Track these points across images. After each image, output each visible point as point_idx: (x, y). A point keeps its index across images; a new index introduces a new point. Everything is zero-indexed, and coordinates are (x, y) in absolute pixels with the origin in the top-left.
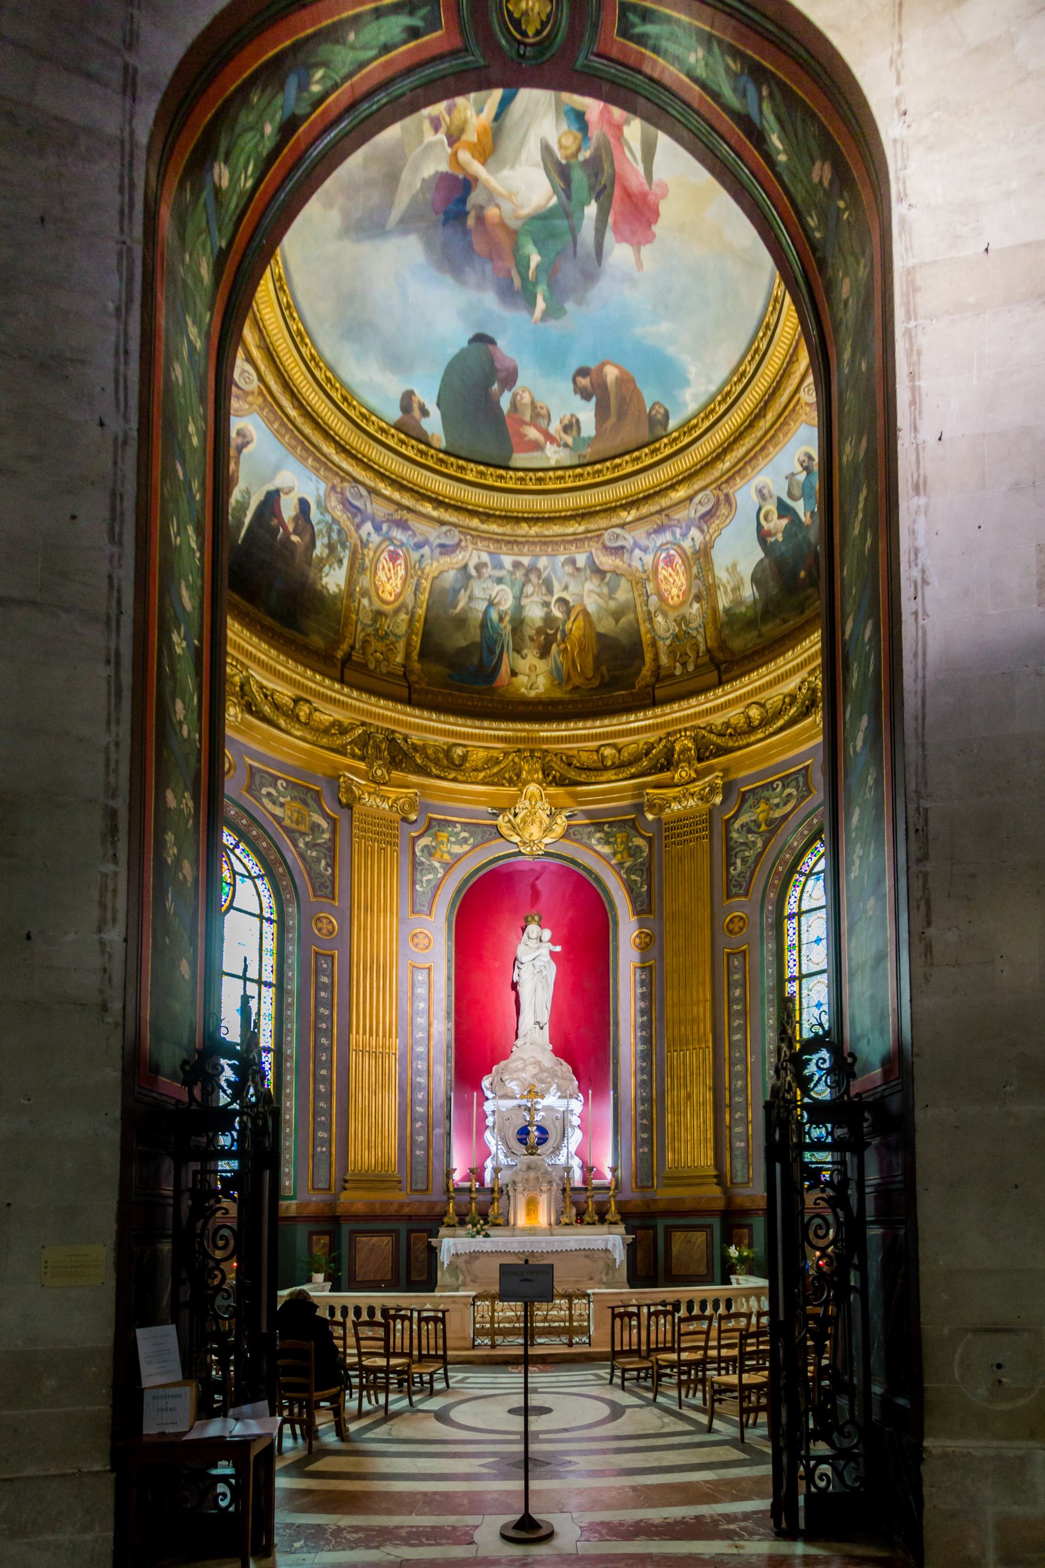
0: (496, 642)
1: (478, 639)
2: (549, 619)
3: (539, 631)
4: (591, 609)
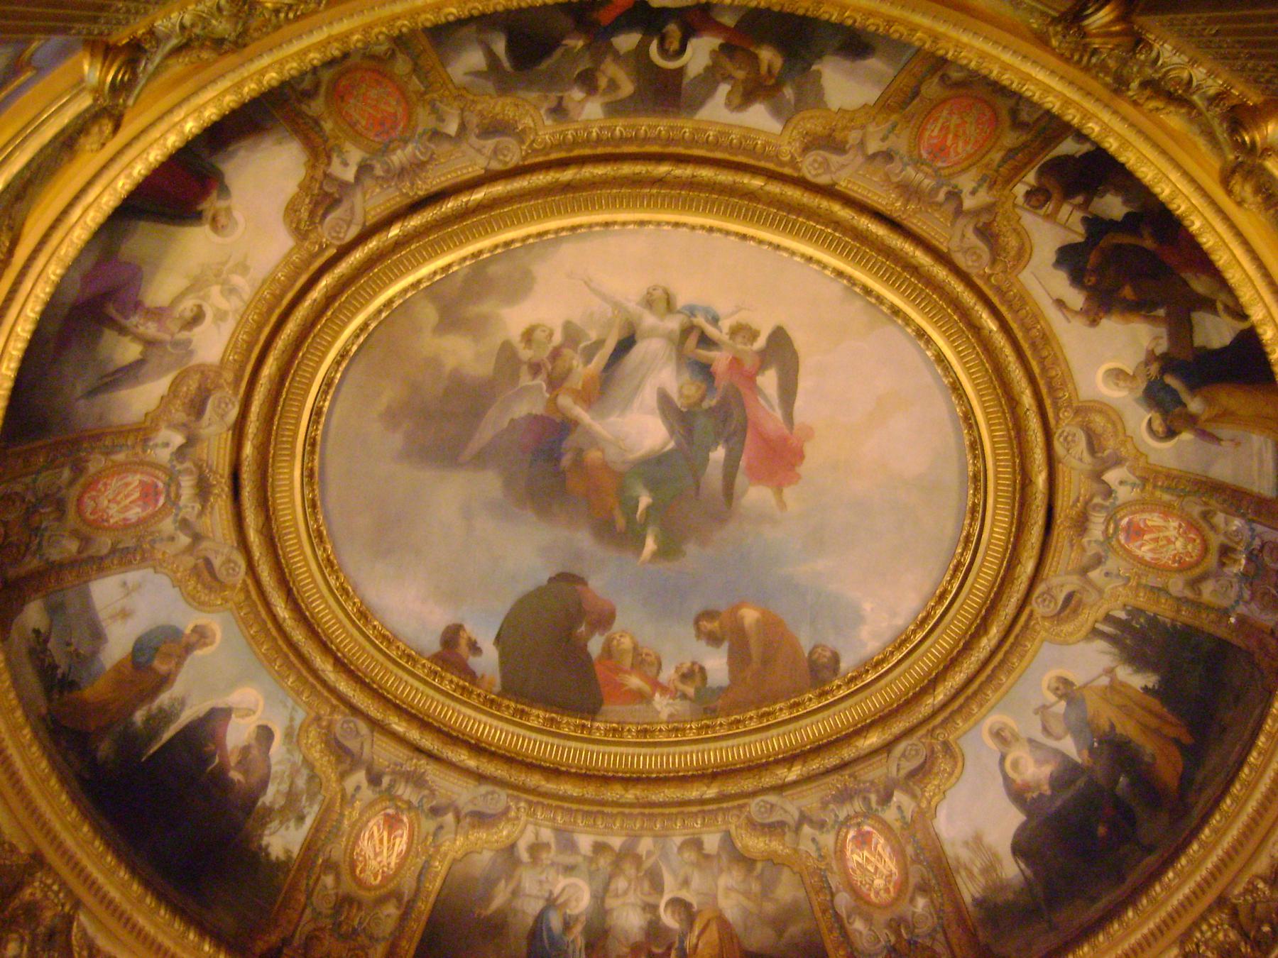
2: (654, 930)
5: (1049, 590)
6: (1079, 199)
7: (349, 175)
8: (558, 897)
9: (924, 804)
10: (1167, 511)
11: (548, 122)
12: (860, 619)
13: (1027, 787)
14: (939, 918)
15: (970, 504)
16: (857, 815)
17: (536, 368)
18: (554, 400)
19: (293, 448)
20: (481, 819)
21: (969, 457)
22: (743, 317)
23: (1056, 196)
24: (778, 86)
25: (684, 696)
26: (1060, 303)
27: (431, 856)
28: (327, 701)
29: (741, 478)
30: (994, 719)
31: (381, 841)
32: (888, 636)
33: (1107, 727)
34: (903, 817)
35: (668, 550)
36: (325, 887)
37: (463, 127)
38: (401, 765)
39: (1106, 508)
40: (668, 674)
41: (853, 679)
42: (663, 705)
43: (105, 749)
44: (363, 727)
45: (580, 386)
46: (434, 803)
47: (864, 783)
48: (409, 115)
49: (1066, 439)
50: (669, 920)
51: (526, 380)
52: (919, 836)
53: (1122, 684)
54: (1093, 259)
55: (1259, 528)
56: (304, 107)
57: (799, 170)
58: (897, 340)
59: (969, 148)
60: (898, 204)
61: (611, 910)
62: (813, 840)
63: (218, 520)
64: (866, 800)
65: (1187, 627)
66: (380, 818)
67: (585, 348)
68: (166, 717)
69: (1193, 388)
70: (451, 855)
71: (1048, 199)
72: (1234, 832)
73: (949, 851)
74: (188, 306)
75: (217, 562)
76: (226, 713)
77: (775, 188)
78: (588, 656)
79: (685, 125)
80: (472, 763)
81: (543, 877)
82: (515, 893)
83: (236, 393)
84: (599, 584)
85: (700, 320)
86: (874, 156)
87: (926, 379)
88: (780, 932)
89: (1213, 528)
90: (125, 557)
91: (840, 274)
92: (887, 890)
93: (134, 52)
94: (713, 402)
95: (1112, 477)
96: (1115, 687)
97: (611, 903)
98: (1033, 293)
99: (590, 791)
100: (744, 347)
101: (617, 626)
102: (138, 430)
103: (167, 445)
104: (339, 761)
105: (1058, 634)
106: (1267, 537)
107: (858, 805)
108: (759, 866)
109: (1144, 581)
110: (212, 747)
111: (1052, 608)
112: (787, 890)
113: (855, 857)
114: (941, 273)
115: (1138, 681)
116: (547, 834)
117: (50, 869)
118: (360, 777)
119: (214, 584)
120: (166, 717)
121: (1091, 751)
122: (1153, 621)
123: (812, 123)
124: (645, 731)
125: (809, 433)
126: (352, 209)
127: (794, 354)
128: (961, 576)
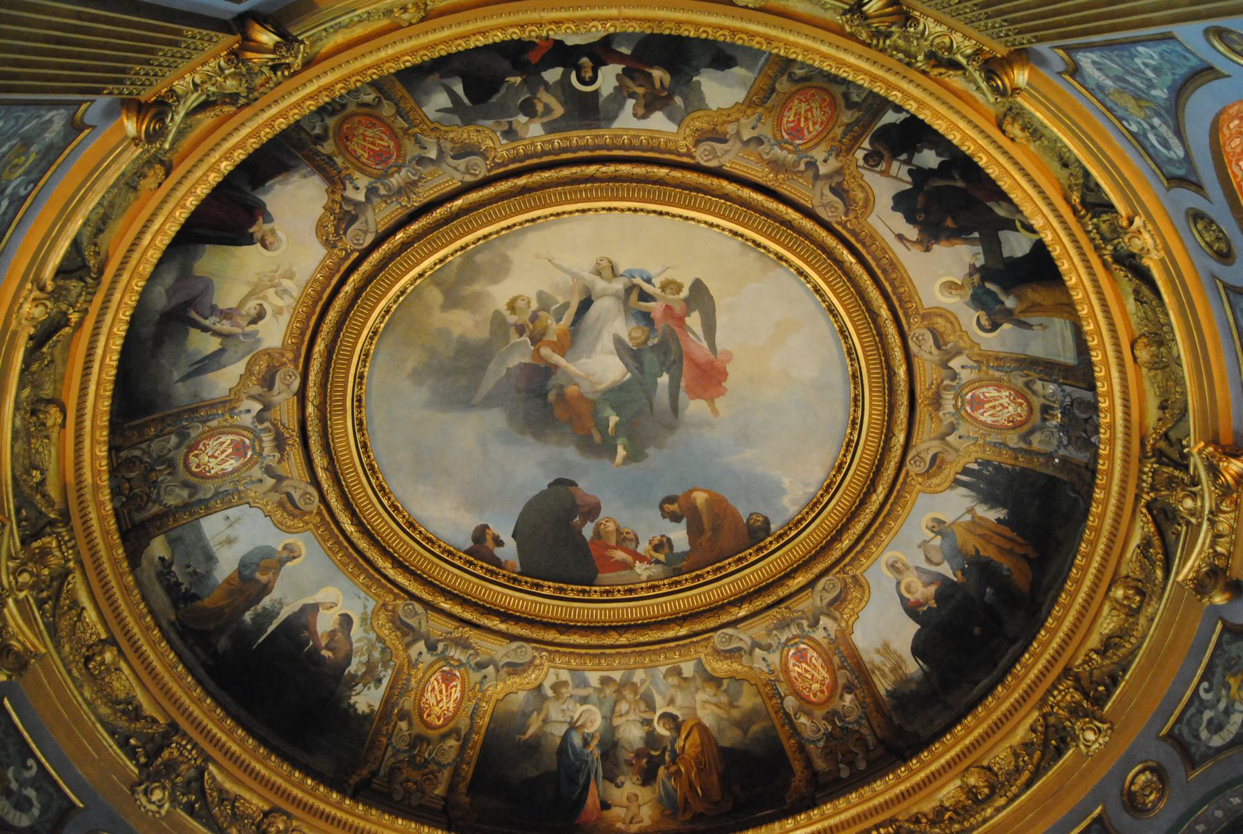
0: (578, 771)
1: (554, 767)
2: (652, 739)
3: (639, 754)
4: (708, 721)
5: (918, 455)
6: (904, 157)
7: (361, 197)
8: (578, 720)
9: (843, 624)
10: (999, 385)
11: (504, 142)
12: (782, 492)
13: (919, 604)
14: (863, 708)
15: (853, 395)
16: (794, 637)
17: (521, 330)
18: (537, 350)
19: (344, 405)
20: (515, 668)
21: (848, 360)
22: (669, 275)
23: (887, 155)
24: (670, 97)
25: (658, 562)
26: (901, 237)
27: (480, 699)
28: (391, 592)
29: (683, 396)
30: (889, 556)
31: (441, 692)
32: (803, 501)
33: (973, 552)
34: (829, 635)
35: (635, 455)
36: (401, 730)
37: (441, 152)
38: (451, 633)
39: (953, 387)
40: (643, 547)
41: (781, 536)
42: (642, 570)
43: (223, 643)
44: (419, 608)
45: (555, 339)
46: (478, 659)
47: (797, 612)
48: (399, 147)
49: (917, 338)
50: (662, 730)
51: (515, 338)
52: (842, 648)
53: (981, 518)
54: (920, 201)
55: (1068, 389)
56: (319, 147)
57: (694, 158)
58: (784, 277)
59: (817, 127)
60: (771, 175)
61: (617, 728)
62: (764, 659)
63: (294, 465)
64: (800, 626)
65: (1023, 470)
66: (438, 675)
67: (557, 309)
68: (269, 615)
69: (1007, 290)
70: (495, 697)
71: (882, 158)
72: (1070, 618)
73: (865, 658)
74: (251, 307)
75: (296, 496)
76: (315, 608)
77: (677, 174)
78: (584, 538)
79: (606, 135)
80: (503, 627)
81: (565, 707)
82: (545, 721)
83: (296, 367)
84: (584, 485)
85: (638, 281)
86: (749, 141)
87: (810, 306)
88: (745, 732)
89: (1034, 393)
90: (227, 499)
91: (736, 234)
92: (822, 692)
93: (160, 108)
94: (656, 341)
95: (955, 364)
96: (976, 522)
97: (617, 721)
98: (880, 231)
99: (593, 640)
100: (672, 297)
101: (602, 515)
102: (225, 402)
103: (248, 411)
104: (405, 635)
105: (930, 486)
106: (1074, 396)
107: (794, 631)
108: (725, 682)
109: (988, 439)
110: (306, 634)
111: (923, 468)
112: (748, 700)
113: (795, 670)
114: (808, 224)
115: (993, 515)
116: (565, 675)
117: (185, 735)
118: (421, 646)
119: (297, 512)
120: (269, 615)
121: (964, 571)
122: (998, 468)
123: (699, 122)
124: (631, 591)
125: (729, 356)
126: (366, 221)
127: (711, 298)
128: (852, 450)
